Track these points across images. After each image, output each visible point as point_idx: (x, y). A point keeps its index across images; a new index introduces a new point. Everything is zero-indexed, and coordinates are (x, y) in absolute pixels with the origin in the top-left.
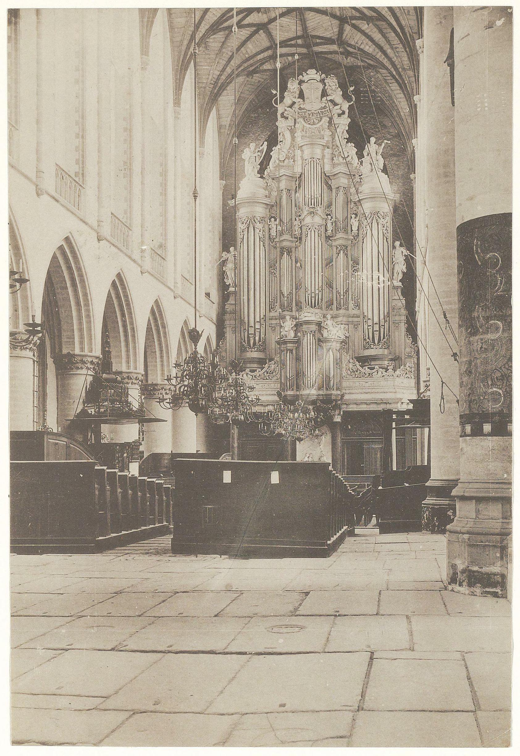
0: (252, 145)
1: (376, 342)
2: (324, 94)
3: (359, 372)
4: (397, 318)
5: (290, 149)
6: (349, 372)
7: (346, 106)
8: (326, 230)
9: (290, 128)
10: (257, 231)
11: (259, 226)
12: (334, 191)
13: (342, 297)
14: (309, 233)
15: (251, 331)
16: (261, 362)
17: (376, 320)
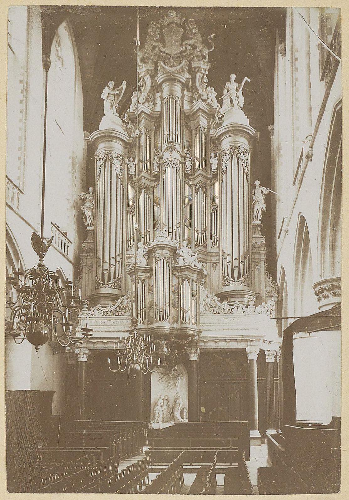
0: (111, 84)
1: (236, 279)
2: (185, 38)
3: (217, 307)
4: (257, 257)
5: (150, 92)
6: (207, 308)
7: (206, 52)
8: (185, 168)
9: (150, 73)
10: (114, 167)
11: (117, 162)
12: (193, 132)
13: (200, 234)
14: (167, 169)
15: (106, 267)
16: (115, 298)
17: (236, 256)
